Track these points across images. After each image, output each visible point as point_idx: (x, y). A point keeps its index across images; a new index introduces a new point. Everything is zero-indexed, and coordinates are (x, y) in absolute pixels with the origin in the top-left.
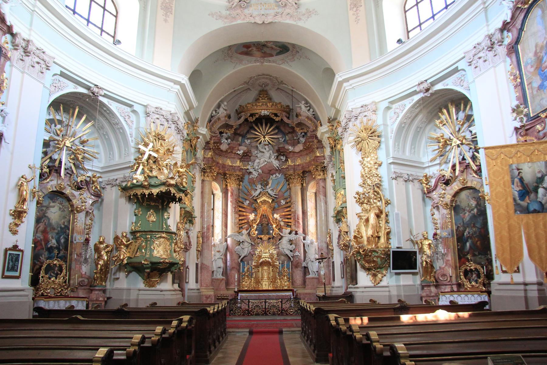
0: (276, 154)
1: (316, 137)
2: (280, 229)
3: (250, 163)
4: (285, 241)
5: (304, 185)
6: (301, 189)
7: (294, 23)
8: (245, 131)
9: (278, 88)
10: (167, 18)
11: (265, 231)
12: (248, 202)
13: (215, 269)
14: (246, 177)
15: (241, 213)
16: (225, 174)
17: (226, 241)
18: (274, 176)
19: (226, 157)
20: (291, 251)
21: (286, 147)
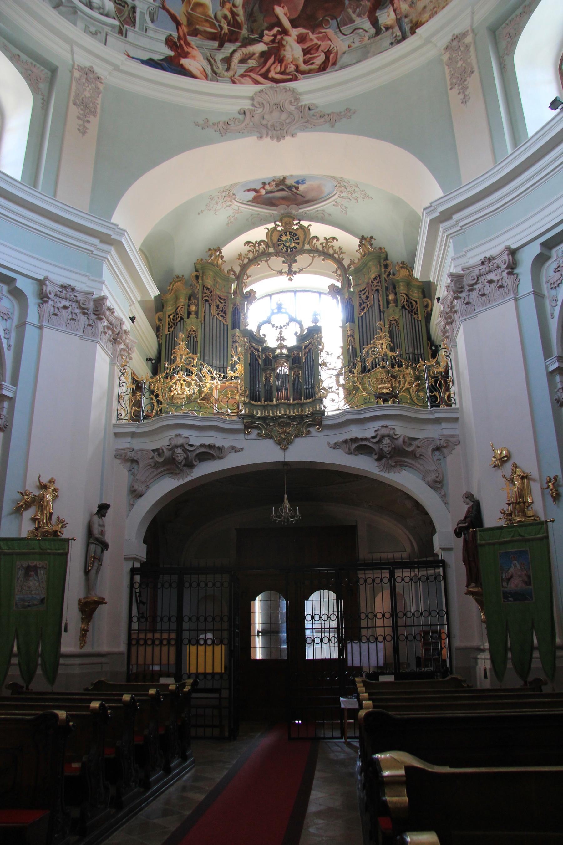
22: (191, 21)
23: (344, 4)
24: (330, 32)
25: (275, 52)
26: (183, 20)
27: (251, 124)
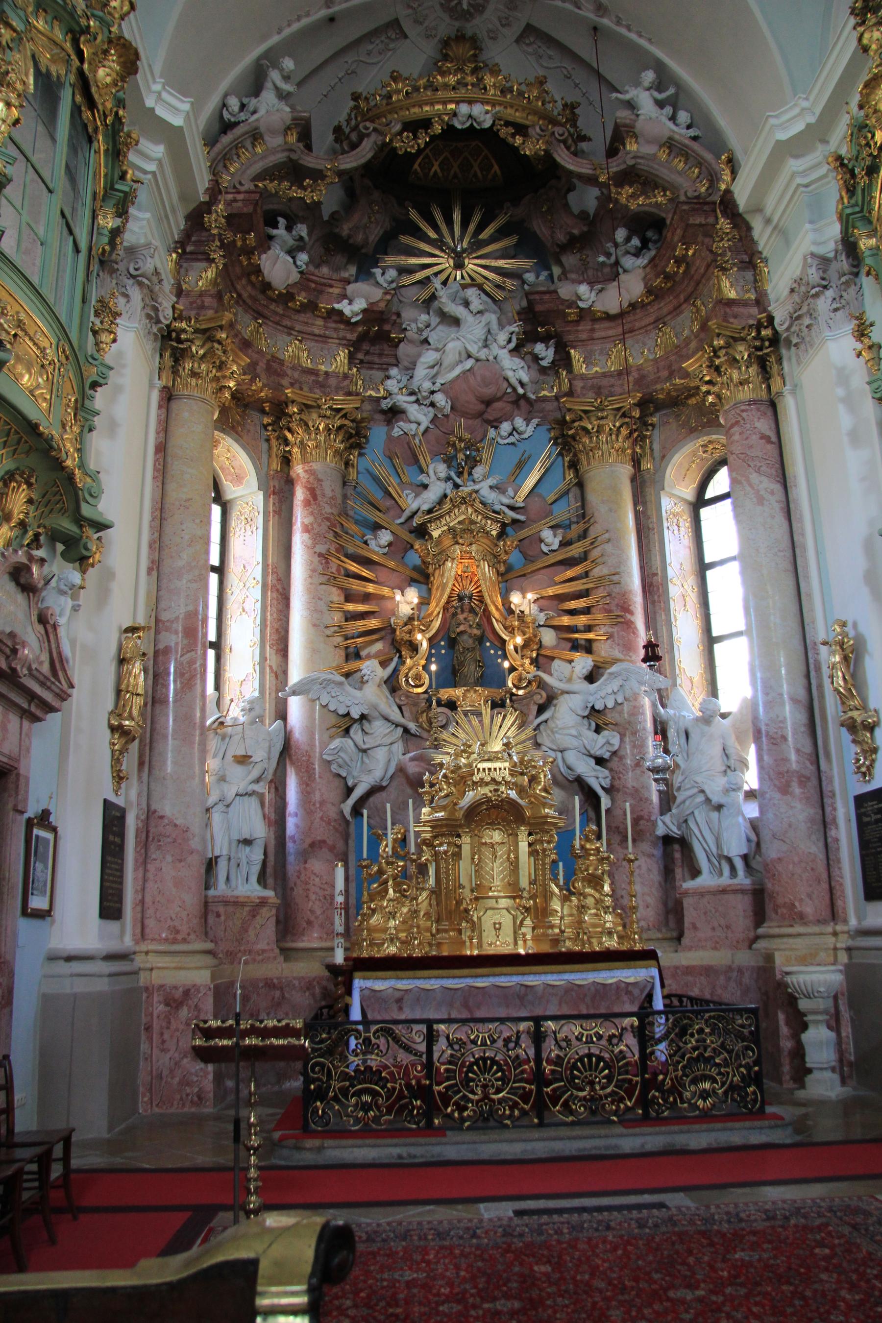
0: (514, 328)
1: (728, 204)
2: (541, 661)
3: (394, 371)
4: (566, 715)
5: (646, 465)
6: (633, 479)
8: (375, 234)
9: (530, 30)
11: (471, 670)
12: (385, 537)
13: (221, 846)
14: (378, 434)
15: (356, 586)
16: (279, 409)
17: (282, 715)
18: (506, 427)
19: (289, 330)
20: (600, 761)
21: (565, 291)
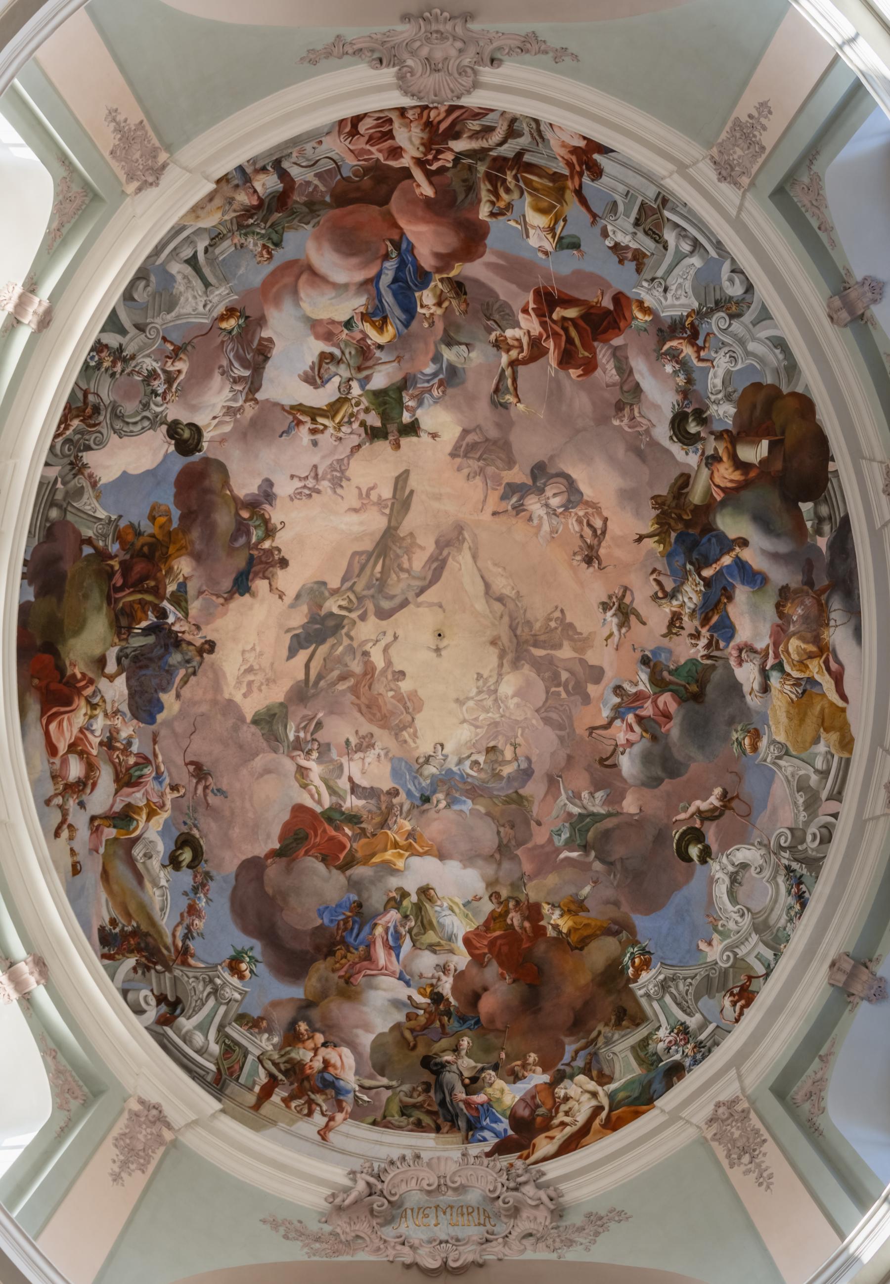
7: (554, 1256)
10: (123, 1175)
22: (559, 193)
23: (331, 196)
24: (351, 161)
25: (436, 136)
26: (570, 196)
27: (481, 44)
